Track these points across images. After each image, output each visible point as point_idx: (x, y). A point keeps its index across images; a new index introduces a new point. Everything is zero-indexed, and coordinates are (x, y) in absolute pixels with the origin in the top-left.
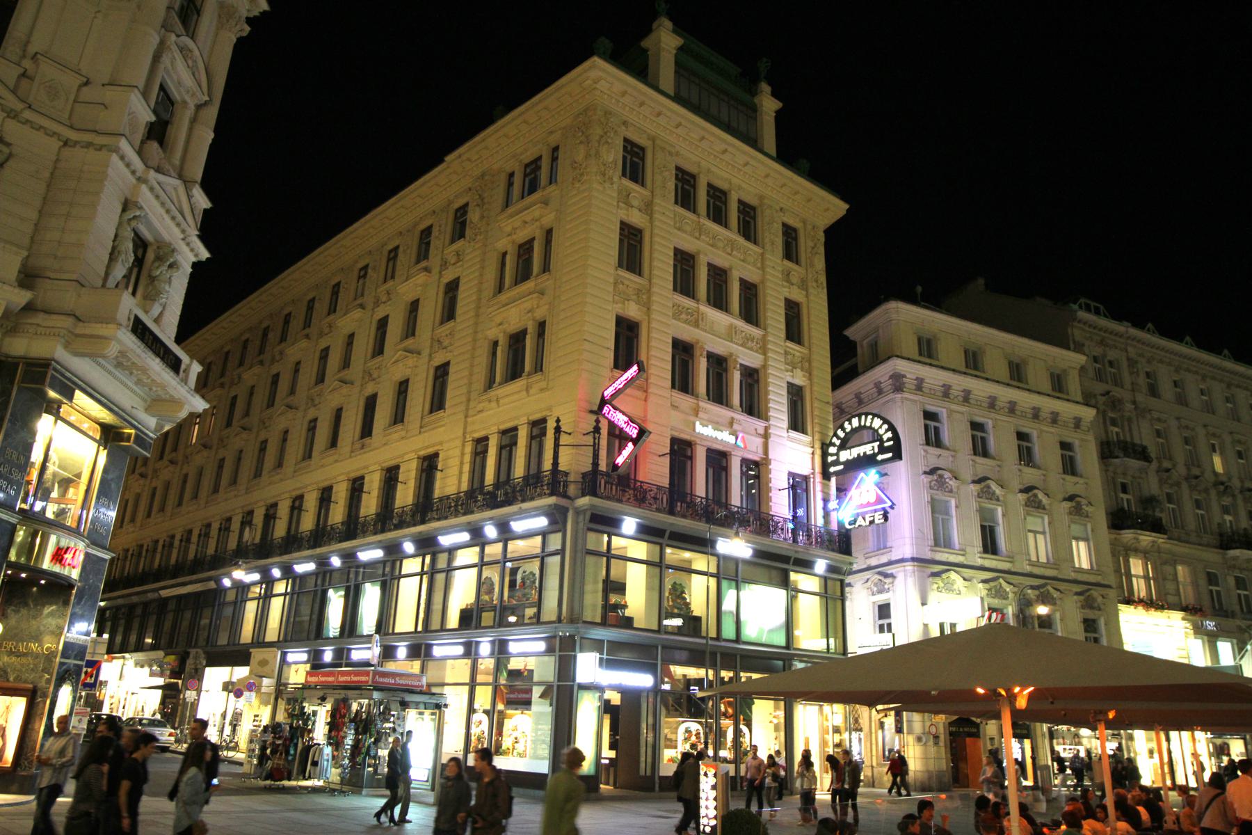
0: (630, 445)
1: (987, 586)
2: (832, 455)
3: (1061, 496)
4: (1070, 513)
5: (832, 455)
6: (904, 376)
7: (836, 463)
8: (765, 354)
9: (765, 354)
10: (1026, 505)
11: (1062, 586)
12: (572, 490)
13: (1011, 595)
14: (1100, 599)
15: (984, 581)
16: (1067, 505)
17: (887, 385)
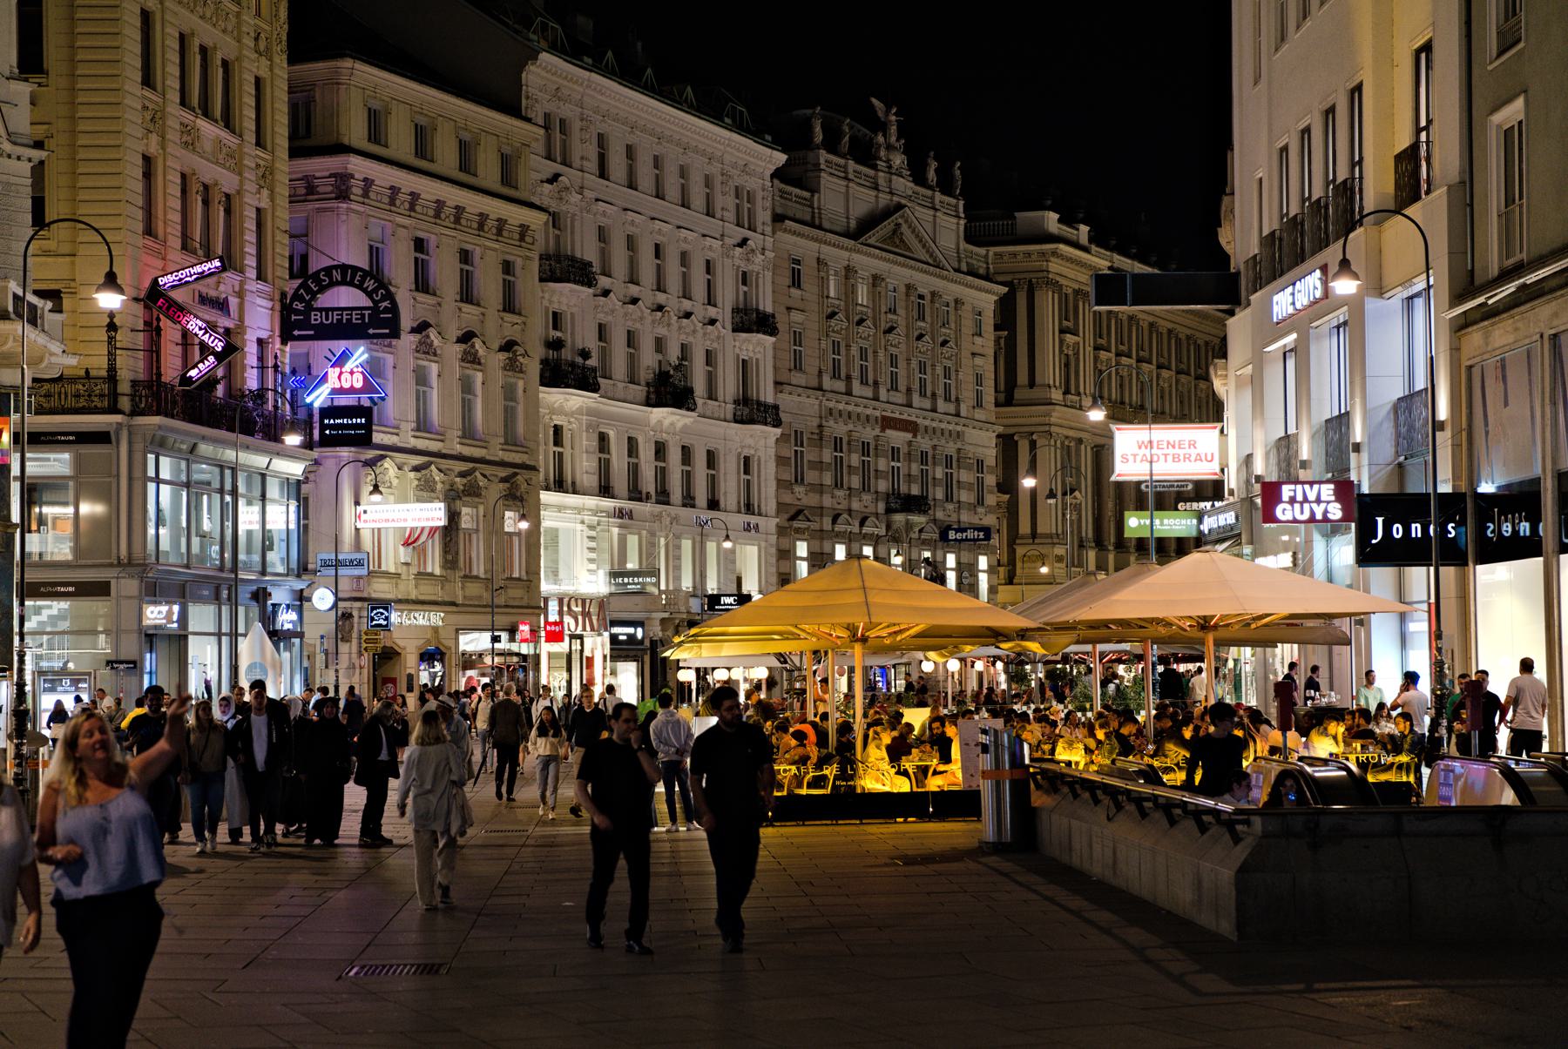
0: (211, 359)
1: (419, 475)
2: (297, 312)
3: (496, 346)
4: (505, 369)
5: (297, 312)
6: (352, 176)
7: (305, 324)
8: (240, 174)
9: (240, 174)
10: (463, 360)
11: (489, 470)
12: (125, 403)
13: (439, 486)
14: (524, 486)
15: (416, 469)
16: (502, 356)
17: (325, 187)
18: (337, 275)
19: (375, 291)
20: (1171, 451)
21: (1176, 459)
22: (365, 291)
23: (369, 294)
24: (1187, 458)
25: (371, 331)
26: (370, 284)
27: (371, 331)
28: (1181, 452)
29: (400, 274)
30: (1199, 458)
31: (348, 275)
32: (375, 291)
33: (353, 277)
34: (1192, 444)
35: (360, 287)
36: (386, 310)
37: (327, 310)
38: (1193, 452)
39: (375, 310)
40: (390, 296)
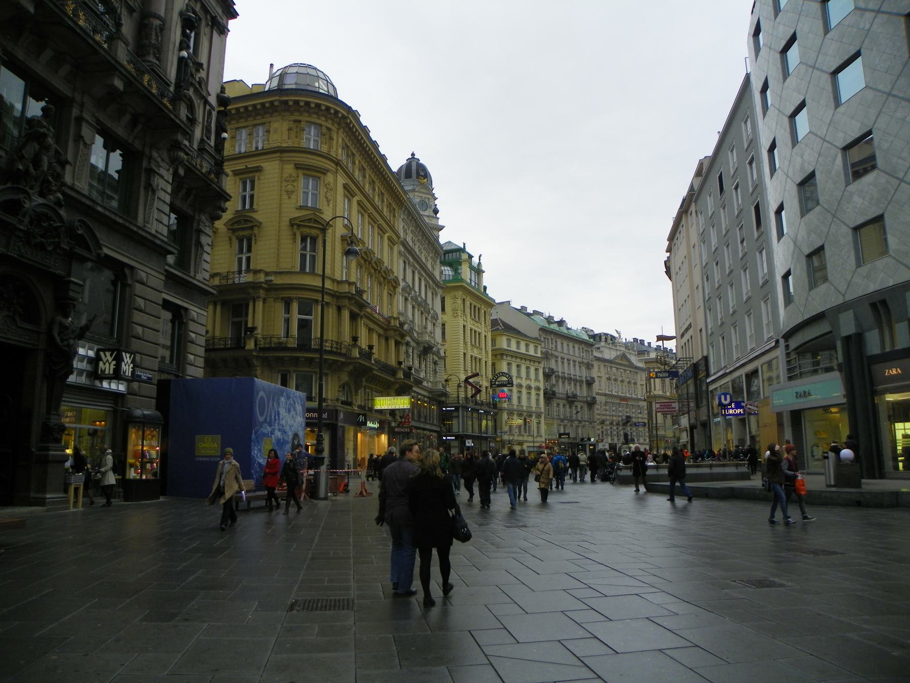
29: (514, 373)
31: (503, 374)
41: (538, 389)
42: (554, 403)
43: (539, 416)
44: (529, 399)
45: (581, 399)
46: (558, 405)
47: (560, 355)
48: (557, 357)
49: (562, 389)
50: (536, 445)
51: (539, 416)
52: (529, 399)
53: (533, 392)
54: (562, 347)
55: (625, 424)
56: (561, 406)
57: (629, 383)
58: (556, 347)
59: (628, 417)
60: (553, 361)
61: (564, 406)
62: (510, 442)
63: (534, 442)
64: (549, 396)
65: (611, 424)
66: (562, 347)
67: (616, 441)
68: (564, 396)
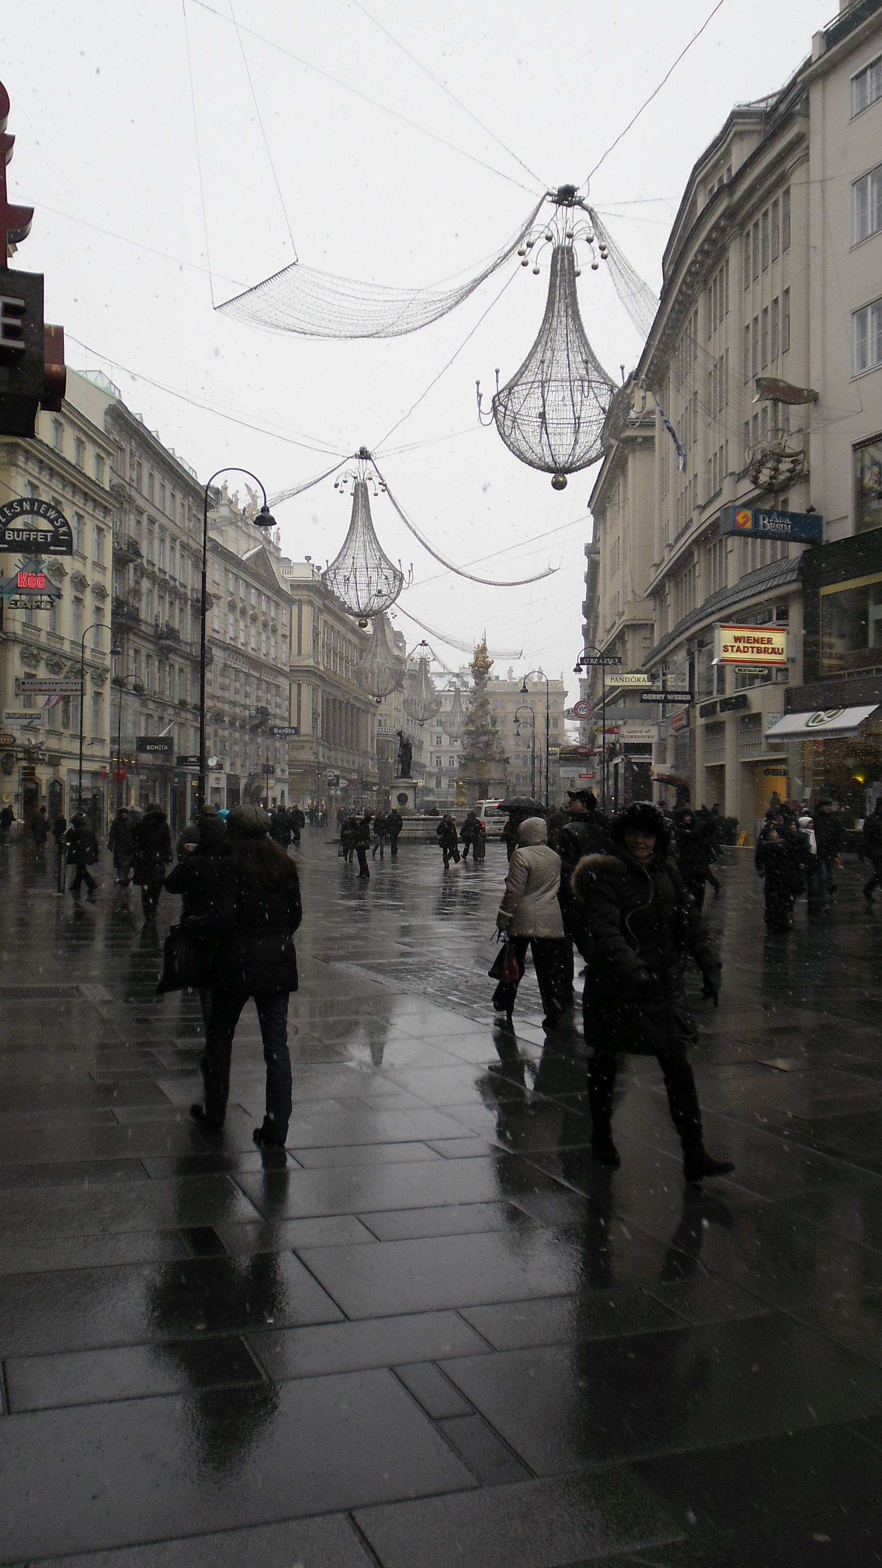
18: (27, 506)
19: (56, 519)
20: (756, 645)
21: (759, 651)
22: (48, 518)
23: (51, 522)
24: (766, 651)
25: (52, 548)
26: (52, 514)
27: (52, 548)
28: (763, 646)
30: (774, 651)
32: (56, 519)
33: (39, 508)
34: (769, 641)
35: (44, 516)
36: (64, 534)
37: (18, 530)
38: (769, 646)
39: (56, 533)
40: (66, 524)
41: (100, 593)
42: (133, 642)
43: (99, 679)
44: (78, 617)
45: (183, 647)
46: (137, 652)
47: (150, 510)
48: (140, 512)
49: (153, 610)
50: (88, 766)
51: (99, 679)
52: (78, 617)
53: (89, 599)
54: (151, 487)
55: (253, 730)
56: (143, 658)
57: (265, 625)
58: (139, 478)
59: (263, 712)
60: (132, 517)
61: (149, 656)
62: (30, 753)
63: (81, 757)
64: (125, 622)
65: (232, 724)
66: (151, 487)
67: (238, 771)
68: (150, 631)
